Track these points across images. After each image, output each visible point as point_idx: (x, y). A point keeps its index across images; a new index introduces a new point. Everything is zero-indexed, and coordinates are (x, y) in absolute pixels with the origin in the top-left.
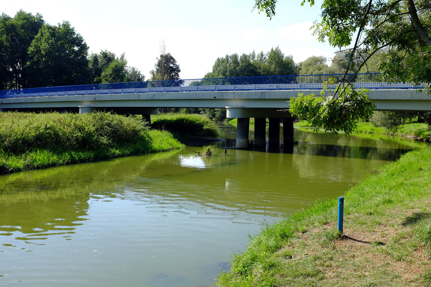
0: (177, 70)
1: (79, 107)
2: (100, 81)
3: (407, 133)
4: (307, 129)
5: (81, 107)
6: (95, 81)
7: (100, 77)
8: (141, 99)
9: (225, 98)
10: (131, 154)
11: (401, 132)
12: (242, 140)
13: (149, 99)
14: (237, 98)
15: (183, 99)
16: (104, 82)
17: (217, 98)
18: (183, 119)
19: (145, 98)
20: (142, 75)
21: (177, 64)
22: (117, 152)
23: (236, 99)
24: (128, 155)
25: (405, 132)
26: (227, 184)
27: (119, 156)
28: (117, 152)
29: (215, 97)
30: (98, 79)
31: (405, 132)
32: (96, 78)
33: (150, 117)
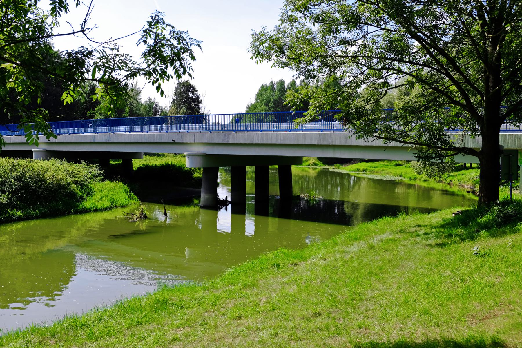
0: (197, 101)
1: (32, 150)
2: (92, 116)
3: (465, 182)
4: (358, 174)
5: (35, 151)
6: (88, 115)
7: (94, 111)
8: (96, 141)
9: (184, 142)
10: (43, 216)
11: (459, 180)
12: (207, 196)
13: (104, 141)
14: (198, 142)
15: (140, 142)
16: (98, 117)
17: (176, 141)
18: (173, 166)
19: (100, 140)
20: (160, 106)
21: (198, 93)
22: (19, 213)
23: (198, 143)
24: (37, 217)
25: (463, 181)
26: (187, 252)
27: (19, 219)
28: (19, 213)
29: (173, 140)
30: (92, 113)
31: (463, 181)
32: (90, 111)
33: (132, 161)
